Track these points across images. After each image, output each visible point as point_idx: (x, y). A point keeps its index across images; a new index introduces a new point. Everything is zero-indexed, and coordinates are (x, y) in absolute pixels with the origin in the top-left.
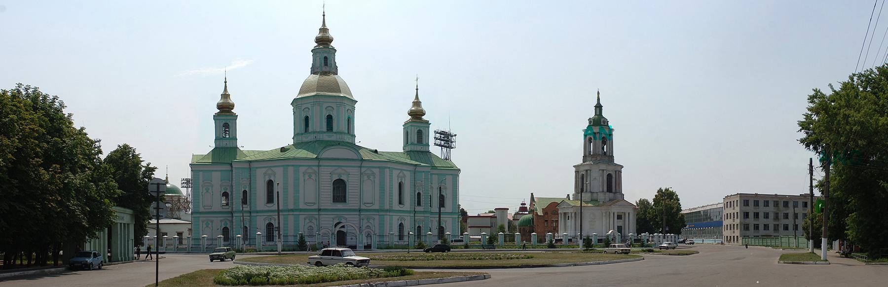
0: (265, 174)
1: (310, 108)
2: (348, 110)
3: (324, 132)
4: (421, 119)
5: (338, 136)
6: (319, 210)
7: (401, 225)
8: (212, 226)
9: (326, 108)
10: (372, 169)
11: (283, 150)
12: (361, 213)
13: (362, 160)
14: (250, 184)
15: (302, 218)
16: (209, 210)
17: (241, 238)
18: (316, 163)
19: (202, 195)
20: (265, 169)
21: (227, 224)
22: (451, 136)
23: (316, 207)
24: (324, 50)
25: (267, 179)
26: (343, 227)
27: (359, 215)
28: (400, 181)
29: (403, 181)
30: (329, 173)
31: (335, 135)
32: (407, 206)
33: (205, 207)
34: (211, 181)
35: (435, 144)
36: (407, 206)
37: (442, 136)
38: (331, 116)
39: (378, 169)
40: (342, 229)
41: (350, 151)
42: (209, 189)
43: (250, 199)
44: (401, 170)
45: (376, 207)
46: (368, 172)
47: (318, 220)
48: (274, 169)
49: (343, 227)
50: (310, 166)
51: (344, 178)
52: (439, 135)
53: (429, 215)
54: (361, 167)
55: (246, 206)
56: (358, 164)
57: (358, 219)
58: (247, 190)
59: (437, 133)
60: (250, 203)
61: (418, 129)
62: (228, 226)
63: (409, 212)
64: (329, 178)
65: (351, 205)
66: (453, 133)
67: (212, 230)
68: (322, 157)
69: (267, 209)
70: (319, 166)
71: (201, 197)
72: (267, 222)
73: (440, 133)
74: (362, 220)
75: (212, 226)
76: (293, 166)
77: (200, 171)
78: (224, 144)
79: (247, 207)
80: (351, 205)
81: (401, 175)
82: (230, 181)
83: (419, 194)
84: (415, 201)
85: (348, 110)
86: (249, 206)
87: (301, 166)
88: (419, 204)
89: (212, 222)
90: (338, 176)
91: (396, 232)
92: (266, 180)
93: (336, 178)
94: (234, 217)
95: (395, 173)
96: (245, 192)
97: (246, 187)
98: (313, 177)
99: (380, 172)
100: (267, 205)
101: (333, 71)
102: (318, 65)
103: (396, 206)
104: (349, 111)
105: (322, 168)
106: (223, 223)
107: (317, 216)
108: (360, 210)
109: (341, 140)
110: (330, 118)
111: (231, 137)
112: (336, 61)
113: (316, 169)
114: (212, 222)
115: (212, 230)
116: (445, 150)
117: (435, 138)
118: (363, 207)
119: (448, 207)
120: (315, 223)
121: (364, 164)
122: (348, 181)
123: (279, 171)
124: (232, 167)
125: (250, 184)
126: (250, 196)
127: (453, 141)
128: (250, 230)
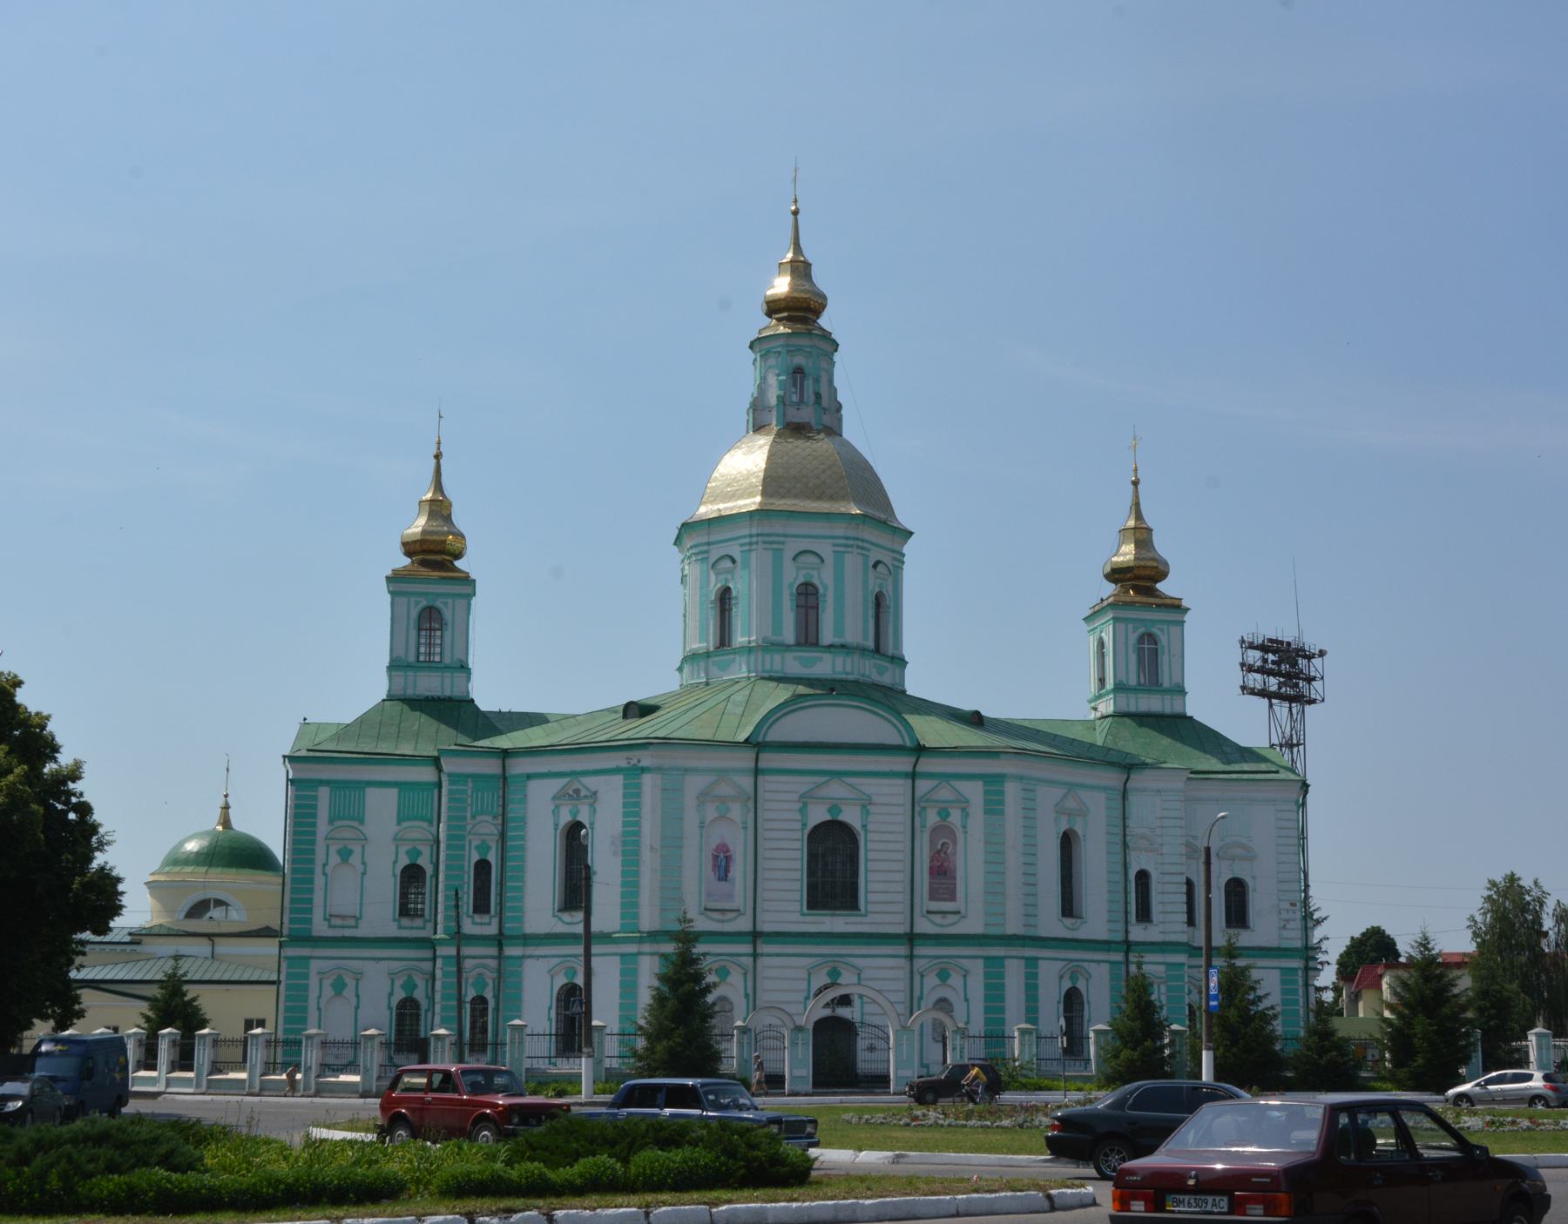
0: (559, 797)
1: (738, 557)
2: (875, 566)
3: (788, 647)
4: (1152, 592)
5: (839, 660)
6: (755, 936)
7: (1072, 1002)
8: (357, 996)
9: (794, 559)
10: (952, 783)
11: (637, 710)
12: (918, 951)
13: (920, 750)
14: (503, 836)
16: (348, 933)
17: (447, 1041)
18: (745, 759)
19: (325, 874)
20: (562, 782)
21: (415, 986)
22: (1305, 657)
23: (744, 924)
24: (794, 341)
25: (565, 818)
26: (845, 1000)
27: (911, 957)
28: (1064, 827)
29: (1079, 829)
30: (796, 797)
31: (827, 657)
32: (1098, 919)
33: (335, 922)
34: (362, 822)
35: (1243, 688)
36: (1098, 919)
37: (1271, 657)
38: (814, 586)
40: (843, 1012)
42: (351, 852)
43: (501, 894)
44: (1071, 786)
45: (973, 925)
46: (944, 794)
47: (750, 977)
48: (587, 781)
49: (845, 1000)
50: (725, 770)
51: (851, 816)
52: (1258, 654)
53: (1181, 958)
54: (913, 776)
55: (486, 918)
56: (903, 763)
57: (902, 974)
58: (492, 857)
59: (1252, 646)
60: (501, 904)
61: (1142, 630)
62: (419, 994)
63: (1105, 945)
64: (799, 817)
65: (877, 918)
66: (1312, 642)
67: (357, 1007)
69: (561, 928)
71: (319, 881)
72: (561, 981)
73: (1263, 648)
74: (917, 978)
75: (357, 996)
76: (659, 769)
77: (321, 782)
78: (429, 684)
79: (490, 924)
80: (877, 918)
81: (1070, 804)
82: (430, 822)
83: (1143, 877)
84: (1126, 903)
85: (875, 566)
86: (495, 921)
87: (687, 770)
88: (1144, 914)
89: (358, 977)
90: (830, 811)
91: (1053, 1020)
92: (560, 827)
93: (818, 815)
94: (439, 962)
95: (1048, 797)
96: (483, 867)
97: (488, 848)
98: (736, 812)
99: (986, 793)
100: (559, 914)
101: (827, 420)
102: (772, 398)
103: (1051, 923)
104: (880, 568)
105: (767, 778)
106: (398, 983)
107: (748, 961)
108: (911, 938)
109: (851, 677)
110: (808, 597)
111: (447, 660)
112: (836, 384)
113: (746, 782)
115: (357, 1007)
116: (1282, 709)
117: (1242, 665)
118: (923, 926)
119: (1264, 929)
120: (742, 985)
121: (927, 765)
122: (864, 826)
123: (611, 791)
124: (440, 770)
125: (503, 836)
126: (501, 884)
127: (1313, 674)
128: (497, 1009)
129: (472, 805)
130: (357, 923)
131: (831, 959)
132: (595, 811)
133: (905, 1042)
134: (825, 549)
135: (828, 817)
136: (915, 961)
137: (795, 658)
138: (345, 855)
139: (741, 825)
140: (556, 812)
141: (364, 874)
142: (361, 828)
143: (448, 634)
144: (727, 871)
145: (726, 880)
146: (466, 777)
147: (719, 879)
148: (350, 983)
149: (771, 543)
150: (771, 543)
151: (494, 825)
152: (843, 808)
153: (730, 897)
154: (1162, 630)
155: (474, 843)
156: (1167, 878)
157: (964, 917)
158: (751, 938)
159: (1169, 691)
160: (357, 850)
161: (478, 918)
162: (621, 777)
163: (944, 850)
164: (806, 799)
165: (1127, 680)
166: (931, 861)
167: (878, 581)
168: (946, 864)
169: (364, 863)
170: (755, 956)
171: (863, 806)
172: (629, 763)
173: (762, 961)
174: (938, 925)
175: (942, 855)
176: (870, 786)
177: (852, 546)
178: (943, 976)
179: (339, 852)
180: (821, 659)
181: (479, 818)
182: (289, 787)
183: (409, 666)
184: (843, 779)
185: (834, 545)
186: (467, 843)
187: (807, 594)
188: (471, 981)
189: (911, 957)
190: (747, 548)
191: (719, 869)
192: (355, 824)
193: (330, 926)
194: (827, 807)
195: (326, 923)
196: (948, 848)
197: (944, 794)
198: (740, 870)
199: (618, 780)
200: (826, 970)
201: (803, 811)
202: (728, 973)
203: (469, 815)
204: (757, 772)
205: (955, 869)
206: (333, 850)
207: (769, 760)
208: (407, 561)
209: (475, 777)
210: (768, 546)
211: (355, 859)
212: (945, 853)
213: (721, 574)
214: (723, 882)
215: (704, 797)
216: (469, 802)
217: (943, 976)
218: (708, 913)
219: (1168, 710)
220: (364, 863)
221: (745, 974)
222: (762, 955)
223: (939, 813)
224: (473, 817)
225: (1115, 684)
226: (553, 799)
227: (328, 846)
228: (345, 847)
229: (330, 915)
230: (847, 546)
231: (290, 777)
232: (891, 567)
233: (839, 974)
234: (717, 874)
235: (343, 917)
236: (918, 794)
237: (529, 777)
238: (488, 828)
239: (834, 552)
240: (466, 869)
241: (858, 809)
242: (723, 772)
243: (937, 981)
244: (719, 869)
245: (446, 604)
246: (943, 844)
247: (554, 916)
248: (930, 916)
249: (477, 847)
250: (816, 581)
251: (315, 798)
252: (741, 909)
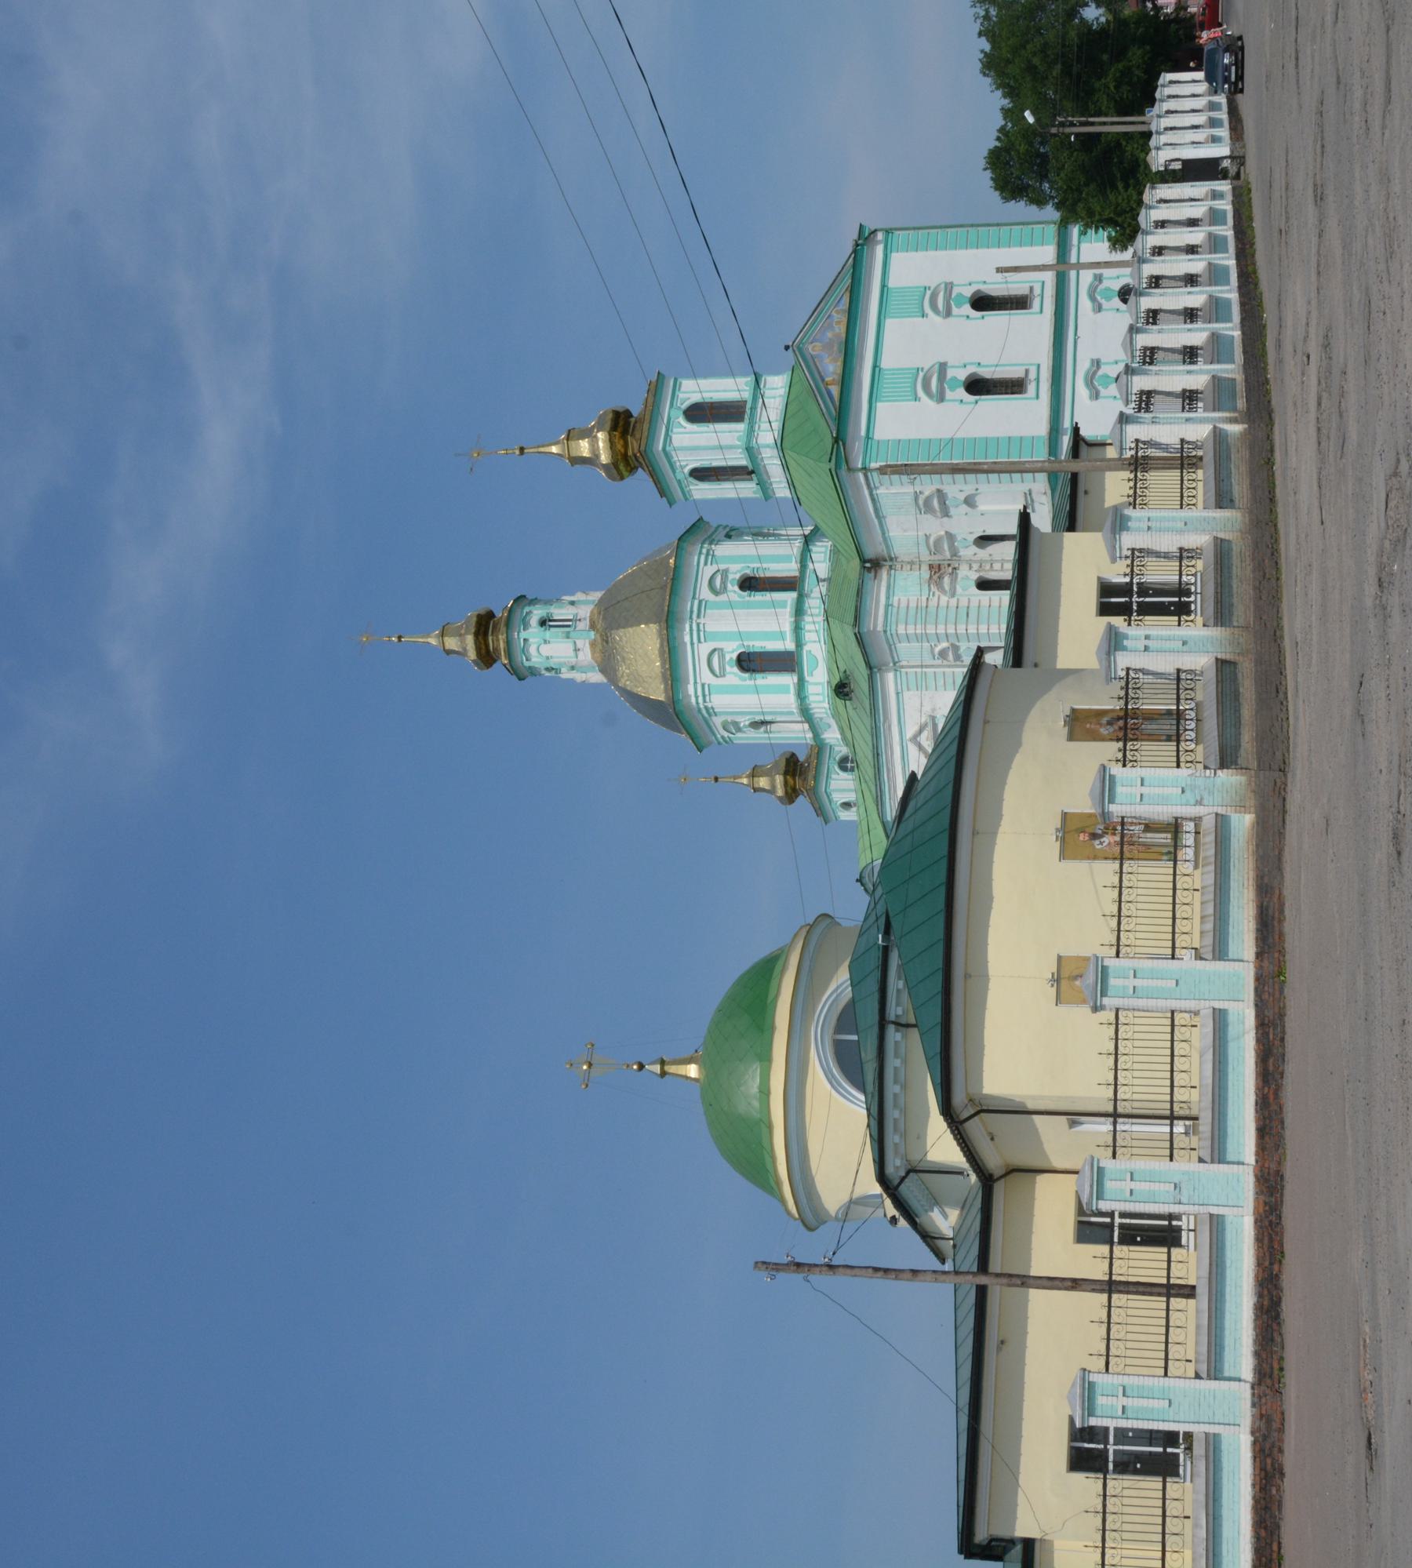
9: (717, 676)
31: (806, 648)
85: (716, 593)
110: (749, 662)
134: (704, 649)
149: (704, 696)
177: (698, 625)
185: (699, 641)
213: (725, 588)
230: (699, 630)
239: (705, 641)
250: (734, 656)
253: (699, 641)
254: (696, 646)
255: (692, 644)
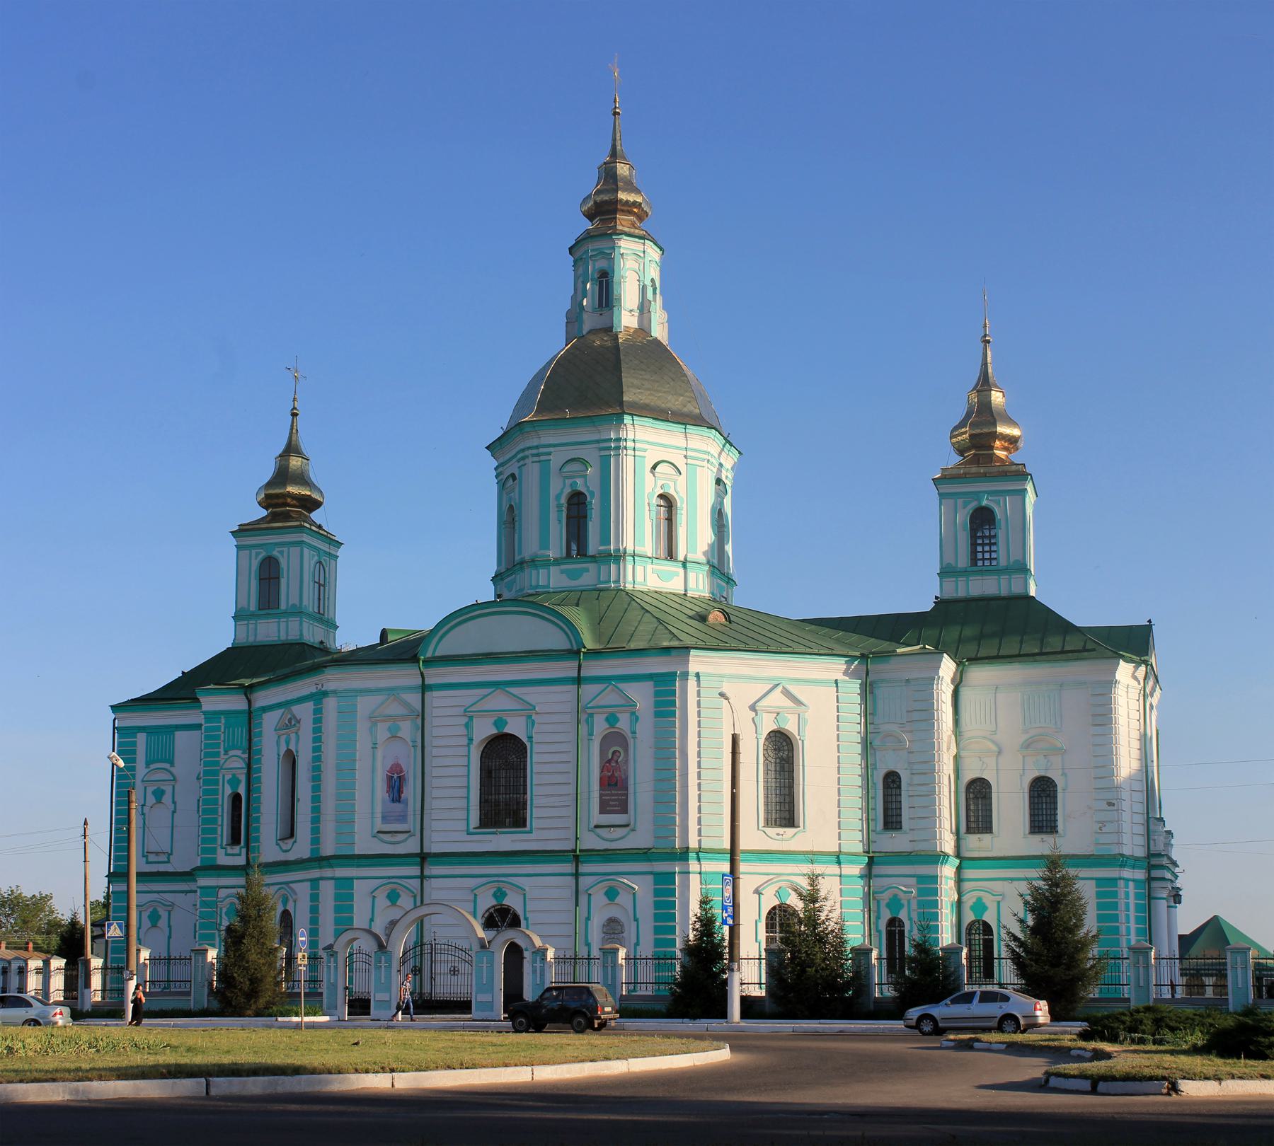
2: (654, 467)
6: (423, 858)
8: (170, 926)
10: (621, 686)
12: (584, 868)
15: (361, 889)
16: (162, 868)
23: (412, 846)
27: (577, 875)
30: (460, 711)
31: (592, 566)
33: (152, 858)
34: (172, 764)
39: (648, 687)
41: (538, 620)
42: (163, 792)
45: (640, 838)
51: (515, 727)
55: (236, 849)
56: (567, 669)
58: (242, 790)
61: (974, 505)
64: (463, 731)
67: (170, 937)
68: (437, 654)
70: (424, 688)
75: (170, 926)
79: (239, 855)
83: (892, 780)
85: (654, 467)
86: (244, 851)
89: (170, 907)
90: (495, 724)
93: (484, 730)
96: (236, 798)
97: (239, 781)
98: (407, 730)
99: (657, 694)
105: (435, 694)
108: (576, 857)
113: (414, 699)
114: (170, 907)
115: (170, 937)
118: (590, 841)
122: (530, 738)
129: (224, 741)
130: (169, 859)
131: (496, 879)
132: (298, 736)
133: (485, 965)
134: (589, 454)
135: (494, 731)
136: (581, 879)
137: (562, 572)
138: (159, 794)
139: (411, 744)
140: (278, 743)
141: (174, 812)
142: (172, 769)
143: (283, 581)
144: (400, 791)
145: (399, 802)
146: (216, 714)
147: (393, 801)
148: (163, 914)
149: (538, 455)
150: (538, 455)
151: (243, 759)
152: (509, 719)
153: (403, 818)
154: (998, 503)
155: (227, 777)
156: (917, 780)
157: (633, 830)
158: (419, 860)
159: (1008, 570)
160: (168, 789)
161: (230, 850)
162: (312, 703)
163: (615, 758)
164: (469, 716)
165: (957, 561)
166: (602, 771)
167: (660, 483)
168: (616, 774)
169: (174, 802)
170: (422, 877)
171: (529, 717)
172: (317, 688)
173: (430, 884)
174: (607, 840)
175: (613, 764)
176: (532, 695)
178: (611, 894)
179: (154, 793)
180: (587, 570)
181: (231, 753)
182: (116, 734)
183: (252, 616)
184: (507, 689)
186: (221, 775)
187: (578, 504)
188: (224, 910)
189: (577, 875)
190: (521, 463)
191: (393, 788)
192: (167, 766)
193: (148, 862)
194: (492, 720)
195: (145, 859)
196: (619, 757)
197: (610, 698)
198: (411, 791)
199: (310, 706)
200: (492, 891)
201: (468, 726)
202: (399, 896)
203: (222, 750)
204: (424, 688)
205: (627, 778)
206: (150, 790)
207: (436, 675)
208: (264, 513)
209: (226, 713)
210: (536, 459)
211: (167, 799)
212: (617, 762)
214: (397, 805)
215: (373, 720)
216: (222, 739)
217: (611, 894)
218: (381, 835)
219: (1004, 593)
220: (174, 802)
221: (415, 897)
222: (430, 877)
223: (607, 720)
224: (226, 752)
225: (942, 568)
226: (275, 730)
227: (145, 788)
228: (158, 788)
229: (147, 852)
231: (116, 726)
232: (683, 468)
233: (504, 895)
234: (392, 795)
235: (157, 853)
236: (584, 700)
237: (265, 709)
238: (235, 762)
240: (220, 803)
241: (522, 720)
242: (391, 691)
243: (605, 900)
244: (393, 788)
245: (281, 552)
246: (614, 752)
247: (277, 844)
248: (598, 830)
249: (228, 781)
251: (134, 744)
252: (412, 830)
253: (601, 449)
254: (597, 445)
255: (598, 442)
